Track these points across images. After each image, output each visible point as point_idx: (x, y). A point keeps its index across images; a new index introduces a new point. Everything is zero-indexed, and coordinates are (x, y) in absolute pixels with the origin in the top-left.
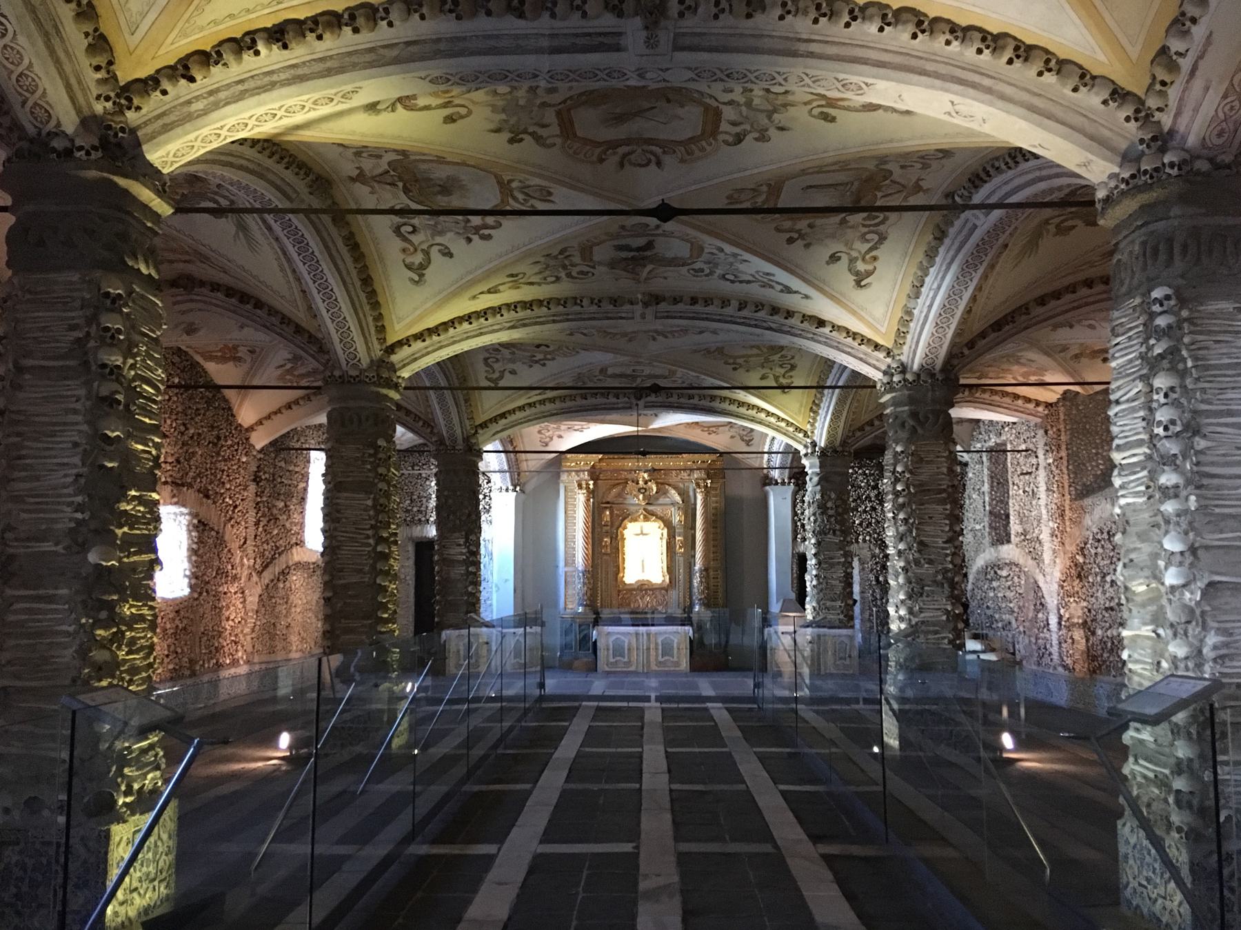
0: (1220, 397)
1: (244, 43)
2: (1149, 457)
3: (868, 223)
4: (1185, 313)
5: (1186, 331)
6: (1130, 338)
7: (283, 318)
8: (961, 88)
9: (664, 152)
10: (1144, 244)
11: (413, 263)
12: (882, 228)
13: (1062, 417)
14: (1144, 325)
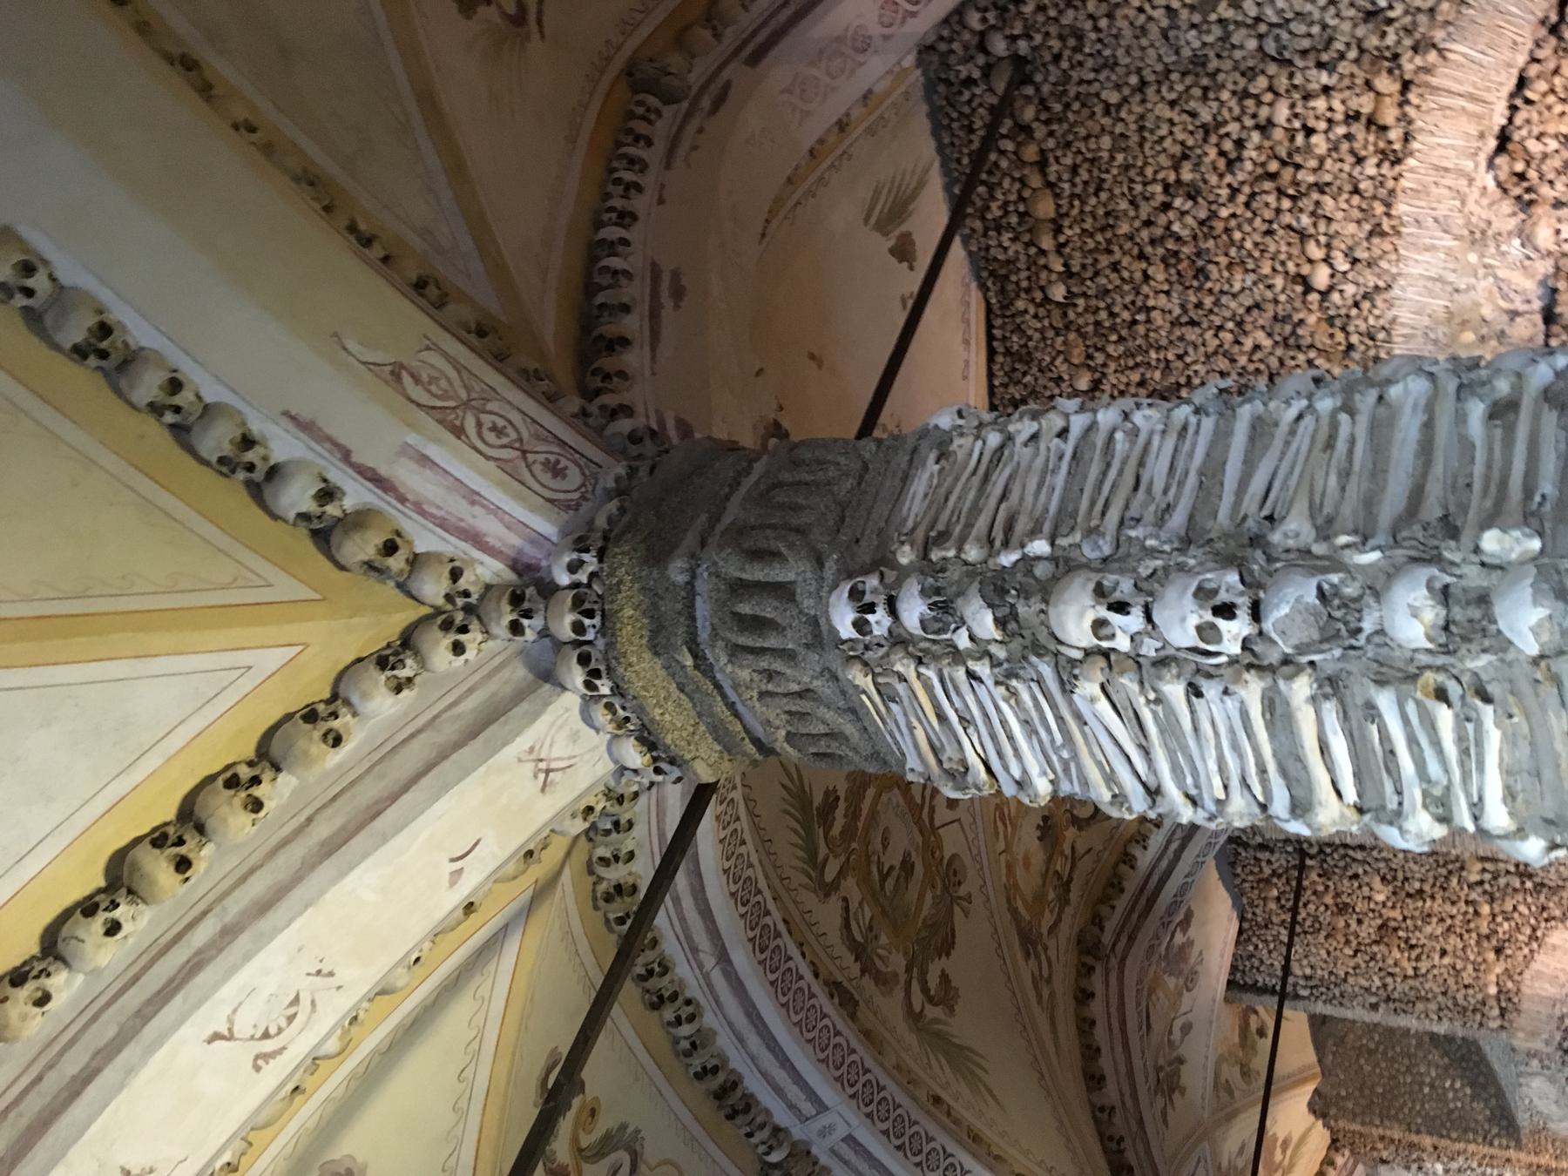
0: (1158, 488)
2: (1331, 686)
4: (906, 556)
5: (951, 553)
6: (966, 721)
8: (178, 1000)
10: (735, 651)
13: (1356, 1127)
14: (920, 662)
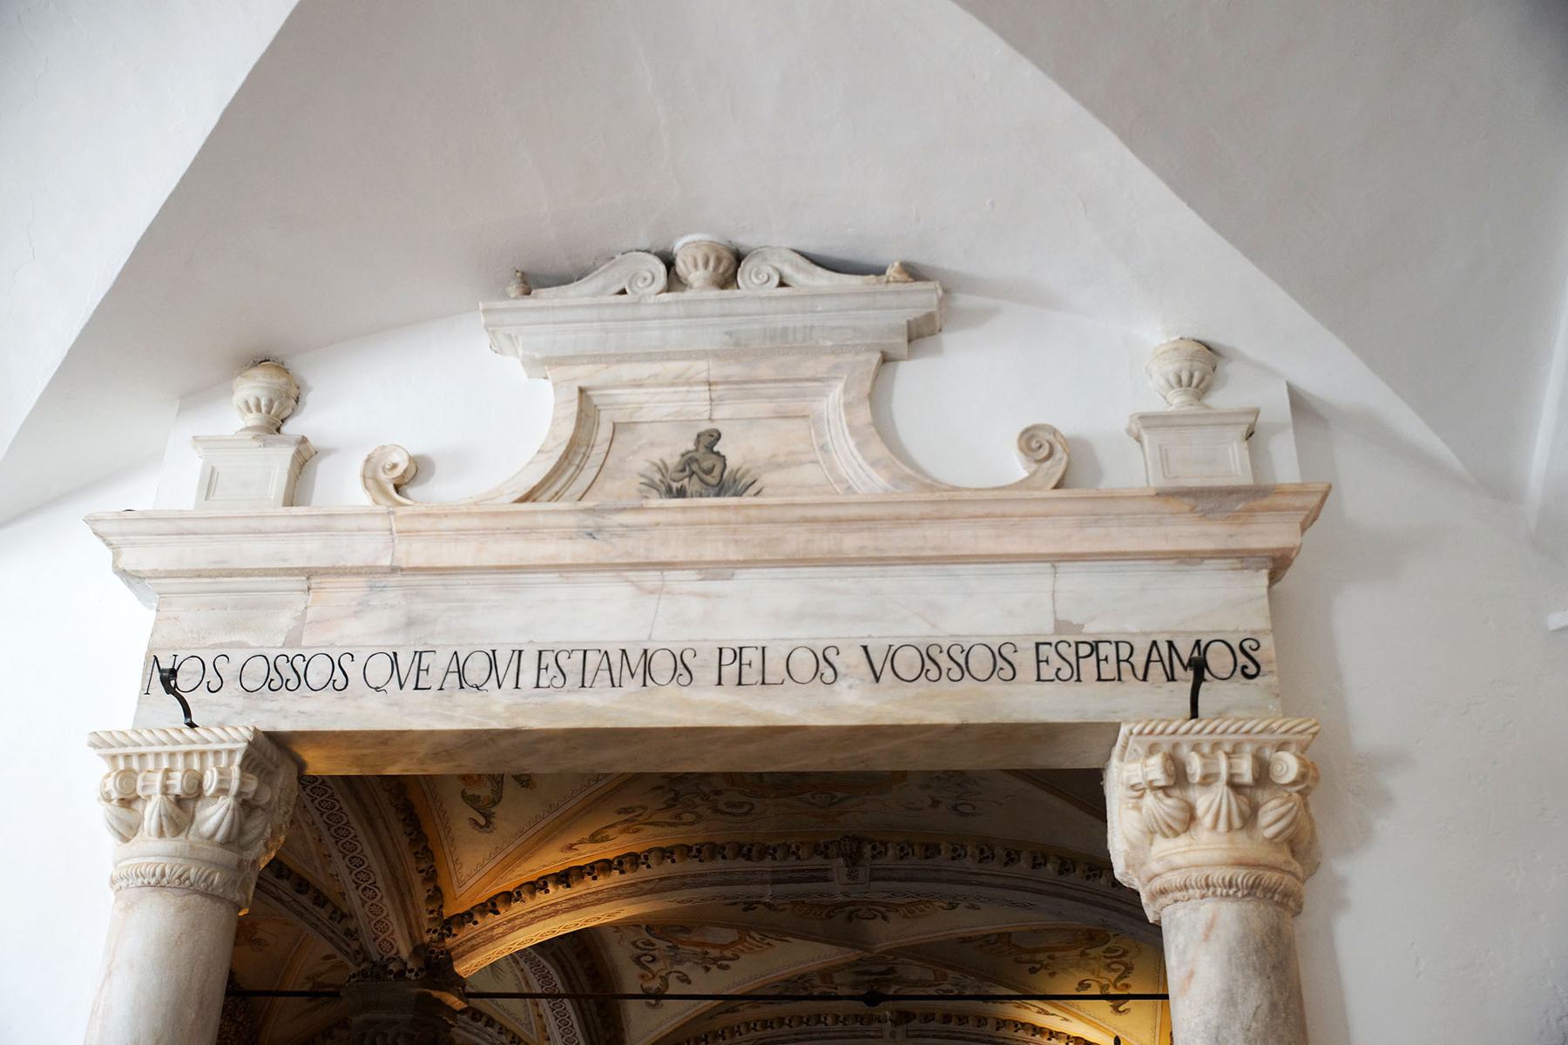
1: (537, 886)
3: (1108, 955)
7: (513, 1038)
9: (888, 911)
11: (651, 988)
12: (1124, 959)
